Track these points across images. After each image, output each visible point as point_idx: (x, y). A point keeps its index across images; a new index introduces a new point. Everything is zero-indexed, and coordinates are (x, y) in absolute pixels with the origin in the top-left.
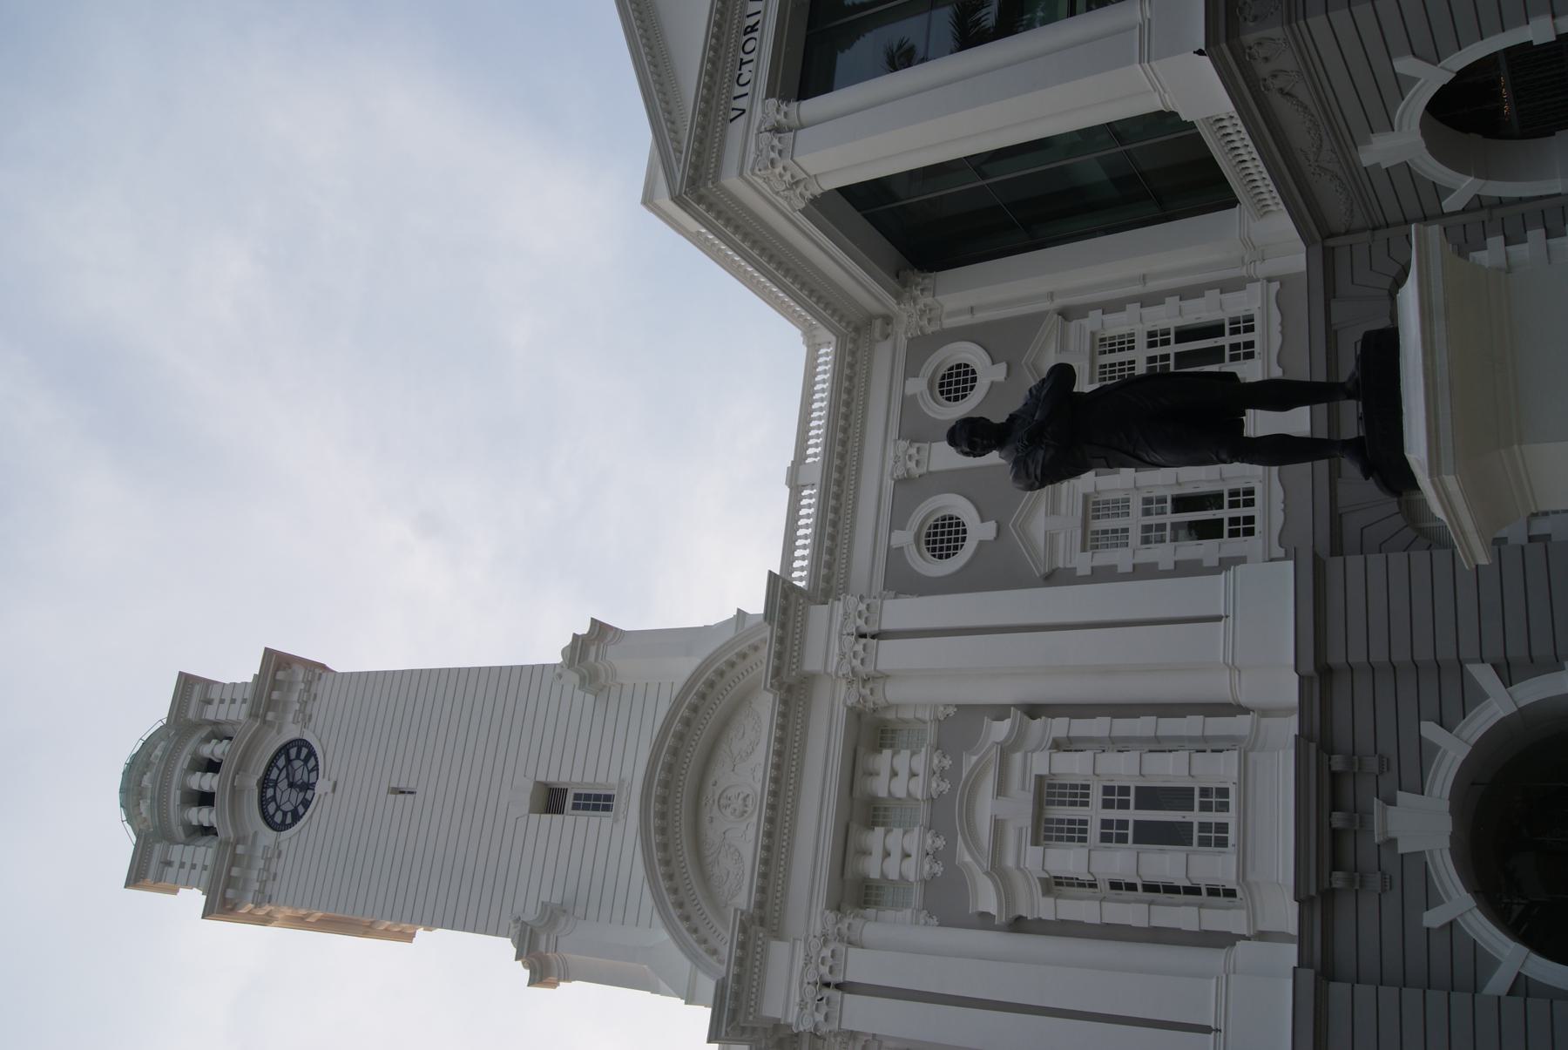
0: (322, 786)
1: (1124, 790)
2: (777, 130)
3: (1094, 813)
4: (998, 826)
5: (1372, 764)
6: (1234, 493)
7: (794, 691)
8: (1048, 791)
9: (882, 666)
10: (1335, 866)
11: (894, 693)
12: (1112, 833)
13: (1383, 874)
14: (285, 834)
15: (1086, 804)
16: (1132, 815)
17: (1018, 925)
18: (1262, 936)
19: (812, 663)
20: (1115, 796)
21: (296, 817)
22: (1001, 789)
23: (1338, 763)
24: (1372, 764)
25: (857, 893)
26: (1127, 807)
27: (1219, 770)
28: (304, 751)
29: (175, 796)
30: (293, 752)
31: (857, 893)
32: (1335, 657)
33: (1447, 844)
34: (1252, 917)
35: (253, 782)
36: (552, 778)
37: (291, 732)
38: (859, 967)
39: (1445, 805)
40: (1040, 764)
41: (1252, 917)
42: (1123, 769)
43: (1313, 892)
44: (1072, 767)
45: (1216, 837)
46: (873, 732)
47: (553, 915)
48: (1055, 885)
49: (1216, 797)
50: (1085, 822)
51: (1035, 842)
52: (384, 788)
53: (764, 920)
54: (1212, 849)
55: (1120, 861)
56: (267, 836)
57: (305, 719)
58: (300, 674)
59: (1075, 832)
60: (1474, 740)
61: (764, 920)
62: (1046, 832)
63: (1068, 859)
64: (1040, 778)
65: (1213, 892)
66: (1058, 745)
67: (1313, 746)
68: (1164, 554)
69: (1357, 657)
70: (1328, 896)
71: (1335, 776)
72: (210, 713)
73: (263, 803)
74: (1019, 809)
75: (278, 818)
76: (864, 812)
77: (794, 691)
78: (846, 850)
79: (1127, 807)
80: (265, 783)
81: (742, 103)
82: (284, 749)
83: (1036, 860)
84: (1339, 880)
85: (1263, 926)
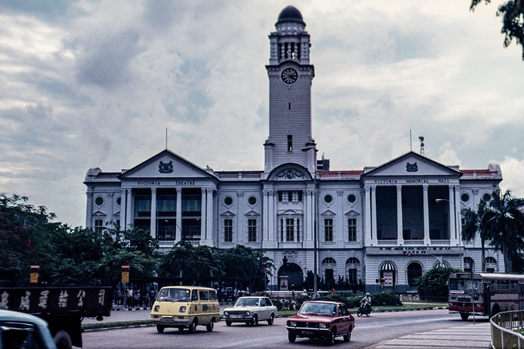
0: (289, 85)
2: (371, 188)
4: (288, 215)
7: (305, 183)
8: (292, 220)
9: (308, 197)
11: (305, 197)
12: (288, 228)
14: (281, 79)
17: (278, 215)
18: (278, 243)
19: (309, 186)
20: (292, 228)
22: (292, 215)
25: (280, 194)
27: (295, 240)
31: (280, 194)
35: (289, 67)
36: (293, 139)
37: (299, 73)
38: (271, 198)
40: (296, 219)
42: (295, 229)
44: (295, 223)
45: (288, 239)
46: (301, 194)
47: (273, 145)
48: (282, 220)
49: (292, 239)
52: (290, 101)
53: (275, 183)
55: (285, 229)
56: (280, 73)
58: (309, 73)
59: (288, 223)
61: (275, 183)
62: (288, 220)
63: (285, 223)
66: (298, 220)
72: (302, 46)
73: (286, 70)
74: (290, 217)
75: (284, 75)
76: (290, 193)
77: (305, 183)
78: (285, 192)
80: (290, 69)
81: (377, 182)
82: (296, 72)
83: (284, 219)
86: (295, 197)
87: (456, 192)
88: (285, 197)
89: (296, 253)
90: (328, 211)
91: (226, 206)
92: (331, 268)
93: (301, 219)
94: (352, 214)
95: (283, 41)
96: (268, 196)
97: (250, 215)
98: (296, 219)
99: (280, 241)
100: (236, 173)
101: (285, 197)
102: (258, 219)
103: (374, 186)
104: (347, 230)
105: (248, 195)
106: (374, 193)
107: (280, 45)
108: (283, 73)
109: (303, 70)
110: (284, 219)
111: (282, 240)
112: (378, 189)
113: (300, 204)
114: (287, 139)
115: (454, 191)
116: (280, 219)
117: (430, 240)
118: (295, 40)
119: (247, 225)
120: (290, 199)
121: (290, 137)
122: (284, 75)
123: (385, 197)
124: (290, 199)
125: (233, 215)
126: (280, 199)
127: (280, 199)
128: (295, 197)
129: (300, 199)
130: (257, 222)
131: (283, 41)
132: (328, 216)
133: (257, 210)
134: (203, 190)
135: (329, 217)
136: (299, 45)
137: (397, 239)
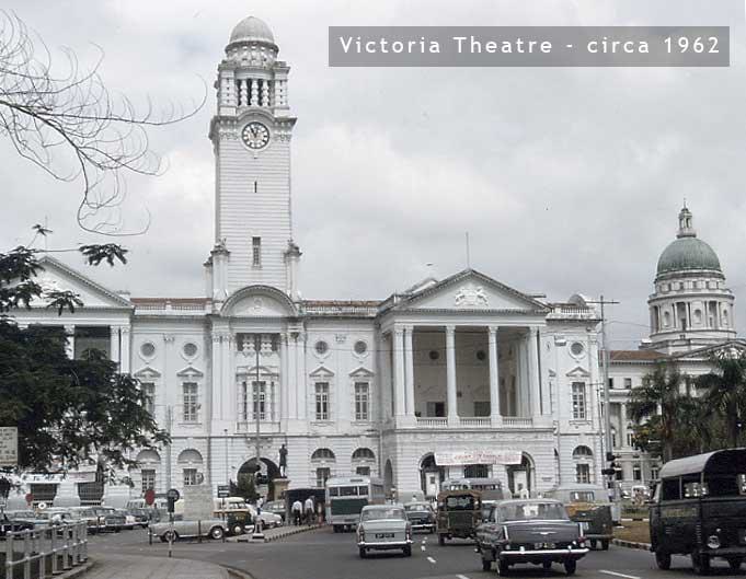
8: (263, 384)
11: (284, 346)
20: (263, 397)
21: (246, 141)
28: (266, 139)
29: (250, 76)
30: (266, 134)
40: (268, 382)
42: (268, 399)
44: (268, 387)
48: (245, 384)
53: (233, 320)
55: (250, 400)
57: (276, 138)
61: (233, 320)
63: (250, 388)
66: (272, 384)
68: (314, 401)
72: (277, 85)
75: (245, 133)
76: (258, 338)
78: (249, 335)
86: (266, 346)
87: (541, 339)
88: (249, 346)
90: (322, 369)
91: (144, 358)
92: (586, 463)
93: (276, 383)
94: (361, 373)
95: (244, 76)
96: (221, 342)
97: (187, 376)
98: (268, 382)
99: (241, 419)
100: (162, 302)
101: (249, 346)
102: (201, 382)
103: (410, 328)
105: (182, 341)
106: (409, 339)
107: (239, 83)
108: (244, 130)
109: (280, 128)
110: (249, 382)
111: (246, 417)
112: (417, 331)
113: (275, 355)
114: (251, 243)
115: (538, 336)
117: (500, 417)
118: (266, 77)
120: (257, 348)
121: (256, 240)
122: (245, 133)
123: (429, 346)
124: (257, 348)
125: (156, 375)
126: (240, 348)
127: (240, 348)
128: (266, 346)
129: (274, 349)
130: (199, 388)
131: (244, 76)
133: (200, 366)
134: (114, 329)
136: (270, 84)
137: (489, 414)
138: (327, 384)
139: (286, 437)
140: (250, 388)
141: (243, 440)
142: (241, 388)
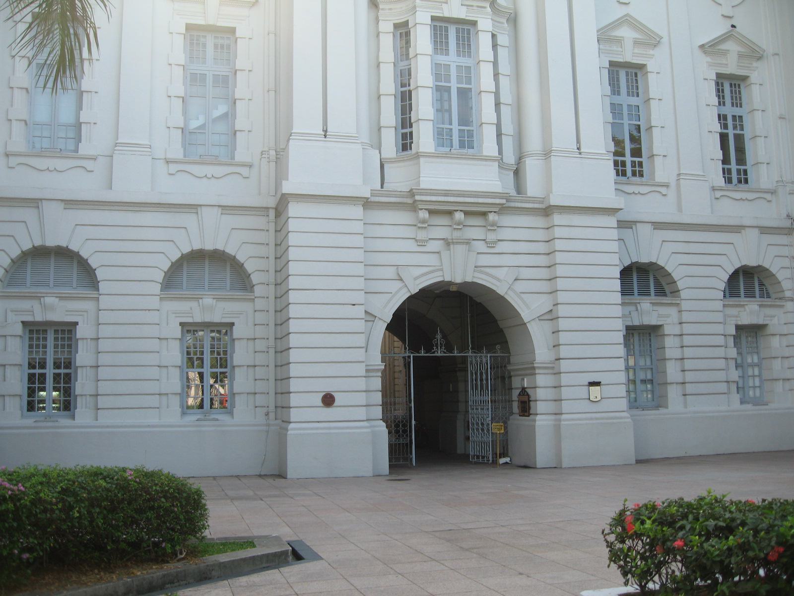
1: (469, 81)
3: (452, 59)
5: (491, 237)
6: (641, 164)
8: (466, 28)
10: (431, 212)
12: (440, 72)
13: (427, 241)
15: (459, 55)
16: (454, 85)
20: (467, 74)
23: (492, 217)
24: (491, 237)
26: (458, 83)
32: (557, 219)
33: (447, 278)
34: (391, 161)
39: (469, 279)
40: (485, 24)
41: (391, 161)
42: (486, 81)
43: (417, 198)
48: (403, 31)
50: (447, 54)
51: (433, 19)
54: (401, 142)
60: (506, 297)
62: (440, 25)
63: (422, 39)
64: (474, 23)
65: (404, 136)
67: (504, 201)
69: (558, 232)
70: (413, 207)
71: (484, 214)
79: (458, 83)
84: (423, 215)
85: (386, 166)
89: (494, 227)
90: (627, 20)
94: (731, 46)
104: (717, 127)
111: (406, 142)
116: (386, 26)
119: (180, 57)
132: (628, 45)
135: (629, 55)
138: (642, 67)
139: (547, 211)
140: (422, 39)
141: (404, 217)
142: (387, 43)
